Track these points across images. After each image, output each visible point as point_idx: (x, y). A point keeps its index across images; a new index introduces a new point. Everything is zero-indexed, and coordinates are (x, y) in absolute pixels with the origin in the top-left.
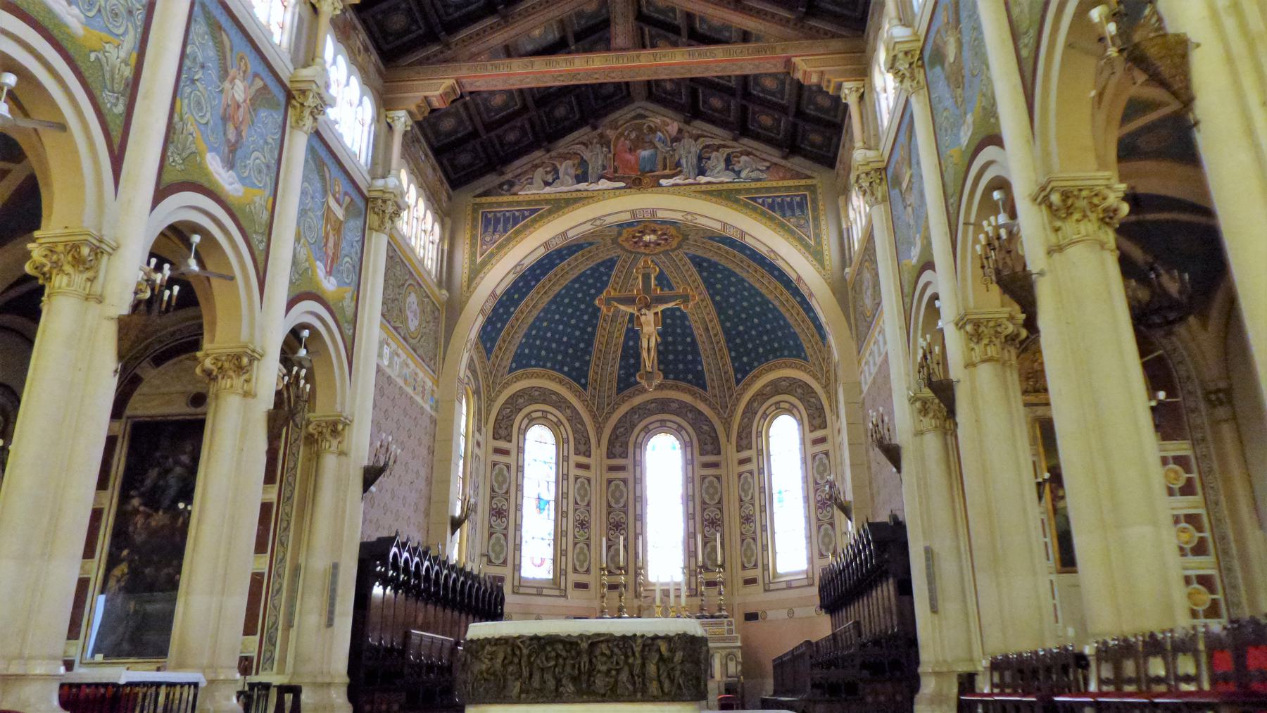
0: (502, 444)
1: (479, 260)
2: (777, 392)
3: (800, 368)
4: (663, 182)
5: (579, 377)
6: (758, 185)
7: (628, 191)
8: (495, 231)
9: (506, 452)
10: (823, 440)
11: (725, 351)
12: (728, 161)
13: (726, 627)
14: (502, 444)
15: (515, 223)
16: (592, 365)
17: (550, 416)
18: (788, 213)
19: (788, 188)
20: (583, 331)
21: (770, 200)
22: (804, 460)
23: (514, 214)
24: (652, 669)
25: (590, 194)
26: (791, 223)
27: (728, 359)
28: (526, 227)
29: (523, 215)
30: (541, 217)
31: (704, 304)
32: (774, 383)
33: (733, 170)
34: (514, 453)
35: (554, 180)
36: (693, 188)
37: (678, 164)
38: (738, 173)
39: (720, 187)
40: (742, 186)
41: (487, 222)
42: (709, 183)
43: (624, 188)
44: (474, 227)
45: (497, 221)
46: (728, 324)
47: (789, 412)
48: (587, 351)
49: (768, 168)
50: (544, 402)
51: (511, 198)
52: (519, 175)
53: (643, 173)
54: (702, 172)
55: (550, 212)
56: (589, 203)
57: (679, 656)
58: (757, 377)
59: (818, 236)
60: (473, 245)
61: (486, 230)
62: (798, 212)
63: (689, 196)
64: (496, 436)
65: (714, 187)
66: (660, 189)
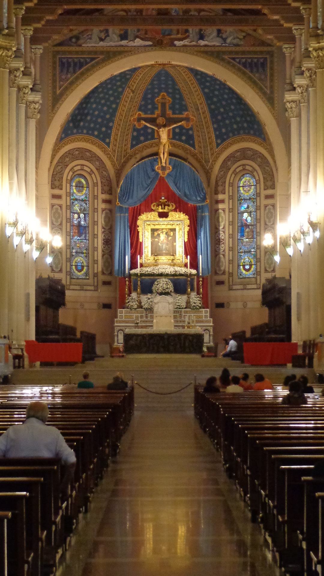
0: (57, 192)
1: (58, 92)
2: (245, 158)
3: (260, 144)
4: (177, 43)
6: (238, 49)
7: (154, 48)
8: (68, 71)
9: (59, 197)
12: (219, 31)
13: (204, 314)
14: (57, 192)
15: (81, 66)
18: (255, 70)
20: (109, 107)
21: (244, 60)
23: (80, 61)
24: (187, 344)
25: (129, 49)
26: (256, 77)
27: (212, 130)
28: (88, 70)
29: (86, 61)
30: (98, 63)
31: (197, 93)
32: (243, 151)
33: (221, 37)
35: (106, 37)
36: (196, 49)
38: (225, 40)
39: (213, 49)
40: (227, 49)
41: (62, 64)
42: (206, 46)
43: (150, 46)
44: (54, 68)
45: (69, 64)
46: (213, 107)
48: (111, 120)
49: (244, 37)
50: (82, 158)
51: (78, 49)
52: (82, 32)
53: (164, 35)
54: (202, 37)
55: (103, 61)
56: (129, 55)
57: (195, 341)
59: (272, 87)
60: (54, 81)
61: (62, 71)
62: (261, 70)
63: (193, 54)
64: (53, 187)
66: (174, 48)
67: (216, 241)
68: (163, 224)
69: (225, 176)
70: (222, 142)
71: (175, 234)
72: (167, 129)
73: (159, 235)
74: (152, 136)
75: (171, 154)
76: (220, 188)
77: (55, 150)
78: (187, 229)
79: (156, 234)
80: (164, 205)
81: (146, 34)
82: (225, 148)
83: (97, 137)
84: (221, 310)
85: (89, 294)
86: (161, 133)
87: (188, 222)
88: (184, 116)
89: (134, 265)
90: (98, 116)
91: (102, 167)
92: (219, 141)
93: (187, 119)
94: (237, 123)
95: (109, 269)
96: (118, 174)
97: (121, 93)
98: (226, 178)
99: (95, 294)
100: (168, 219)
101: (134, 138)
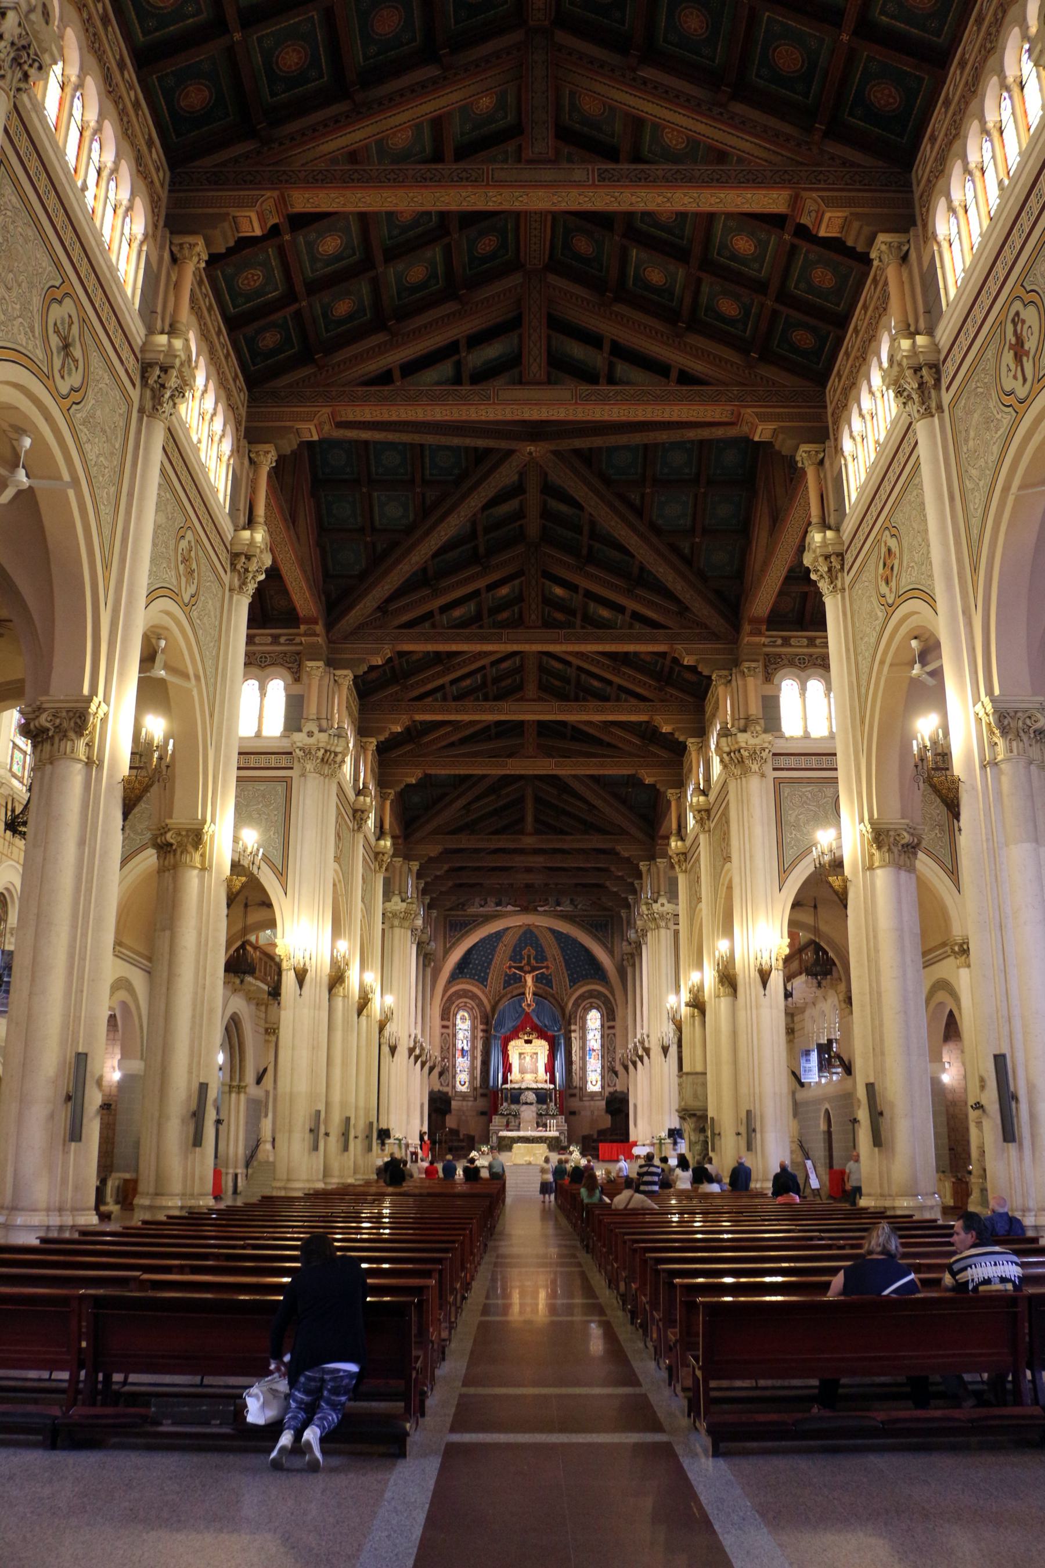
0: (446, 1023)
2: (591, 997)
5: (483, 981)
12: (572, 901)
14: (446, 1023)
20: (487, 957)
27: (566, 975)
30: (479, 924)
32: (590, 991)
38: (576, 907)
44: (445, 927)
47: (597, 1009)
48: (488, 967)
54: (558, 904)
60: (445, 938)
61: (451, 930)
64: (443, 1019)
67: (569, 1062)
69: (576, 1012)
74: (519, 980)
75: (534, 994)
76: (573, 1021)
77: (445, 991)
78: (547, 1053)
80: (530, 1034)
82: (576, 990)
84: (572, 1118)
85: (470, 1104)
87: (547, 1047)
89: (505, 1081)
91: (480, 1004)
93: (547, 968)
96: (494, 1008)
101: (505, 982)
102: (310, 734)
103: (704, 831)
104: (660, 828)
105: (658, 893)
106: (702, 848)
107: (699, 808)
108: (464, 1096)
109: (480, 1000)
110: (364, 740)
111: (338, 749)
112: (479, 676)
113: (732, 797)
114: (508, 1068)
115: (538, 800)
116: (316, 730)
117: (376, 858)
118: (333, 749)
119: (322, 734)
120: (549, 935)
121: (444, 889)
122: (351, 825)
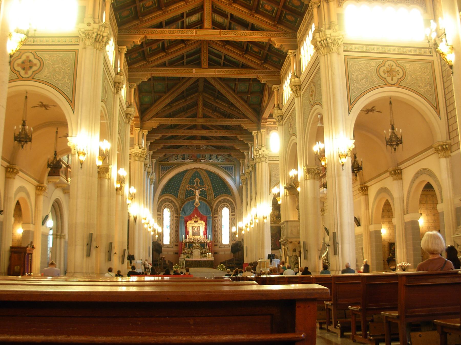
1: (160, 177)
3: (230, 197)
5: (176, 195)
6: (223, 163)
7: (194, 162)
8: (164, 170)
9: (160, 215)
10: (234, 215)
11: (212, 190)
12: (216, 157)
16: (179, 192)
17: (169, 205)
18: (229, 170)
19: (229, 164)
20: (178, 184)
22: (230, 219)
24: (208, 264)
25: (185, 163)
26: (229, 173)
27: (213, 193)
28: (171, 170)
30: (174, 168)
32: (224, 200)
33: (217, 159)
34: (162, 215)
37: (205, 157)
38: (218, 160)
39: (214, 163)
40: (219, 163)
41: (162, 168)
43: (192, 162)
44: (159, 169)
46: (213, 184)
47: (227, 207)
49: (225, 159)
51: (168, 163)
52: (169, 157)
54: (211, 159)
56: (185, 165)
58: (220, 197)
60: (159, 173)
61: (162, 170)
62: (231, 170)
63: (207, 165)
64: (158, 212)
65: (213, 163)
68: (196, 225)
69: (218, 208)
70: (217, 196)
71: (200, 228)
72: (198, 190)
73: (194, 228)
74: (193, 194)
76: (216, 213)
77: (159, 199)
79: (193, 228)
80: (196, 218)
81: (191, 158)
82: (218, 198)
83: (173, 194)
84: (216, 255)
86: (196, 192)
87: (204, 224)
88: (204, 186)
90: (174, 188)
92: (215, 196)
93: (205, 187)
94: (222, 190)
95: (177, 240)
97: (182, 180)
98: (218, 209)
99: (172, 249)
100: (198, 223)
102: (89, 24)
103: (298, 96)
104: (262, 116)
105: (262, 146)
106: (296, 104)
107: (295, 84)
108: (168, 246)
109: (174, 202)
110: (120, 47)
111: (105, 34)
112: (180, 22)
113: (322, 65)
114: (187, 233)
115: (204, 105)
116: (92, 22)
117: (126, 117)
118: (101, 33)
119: (95, 24)
120: (205, 173)
121: (159, 148)
122: (113, 90)
